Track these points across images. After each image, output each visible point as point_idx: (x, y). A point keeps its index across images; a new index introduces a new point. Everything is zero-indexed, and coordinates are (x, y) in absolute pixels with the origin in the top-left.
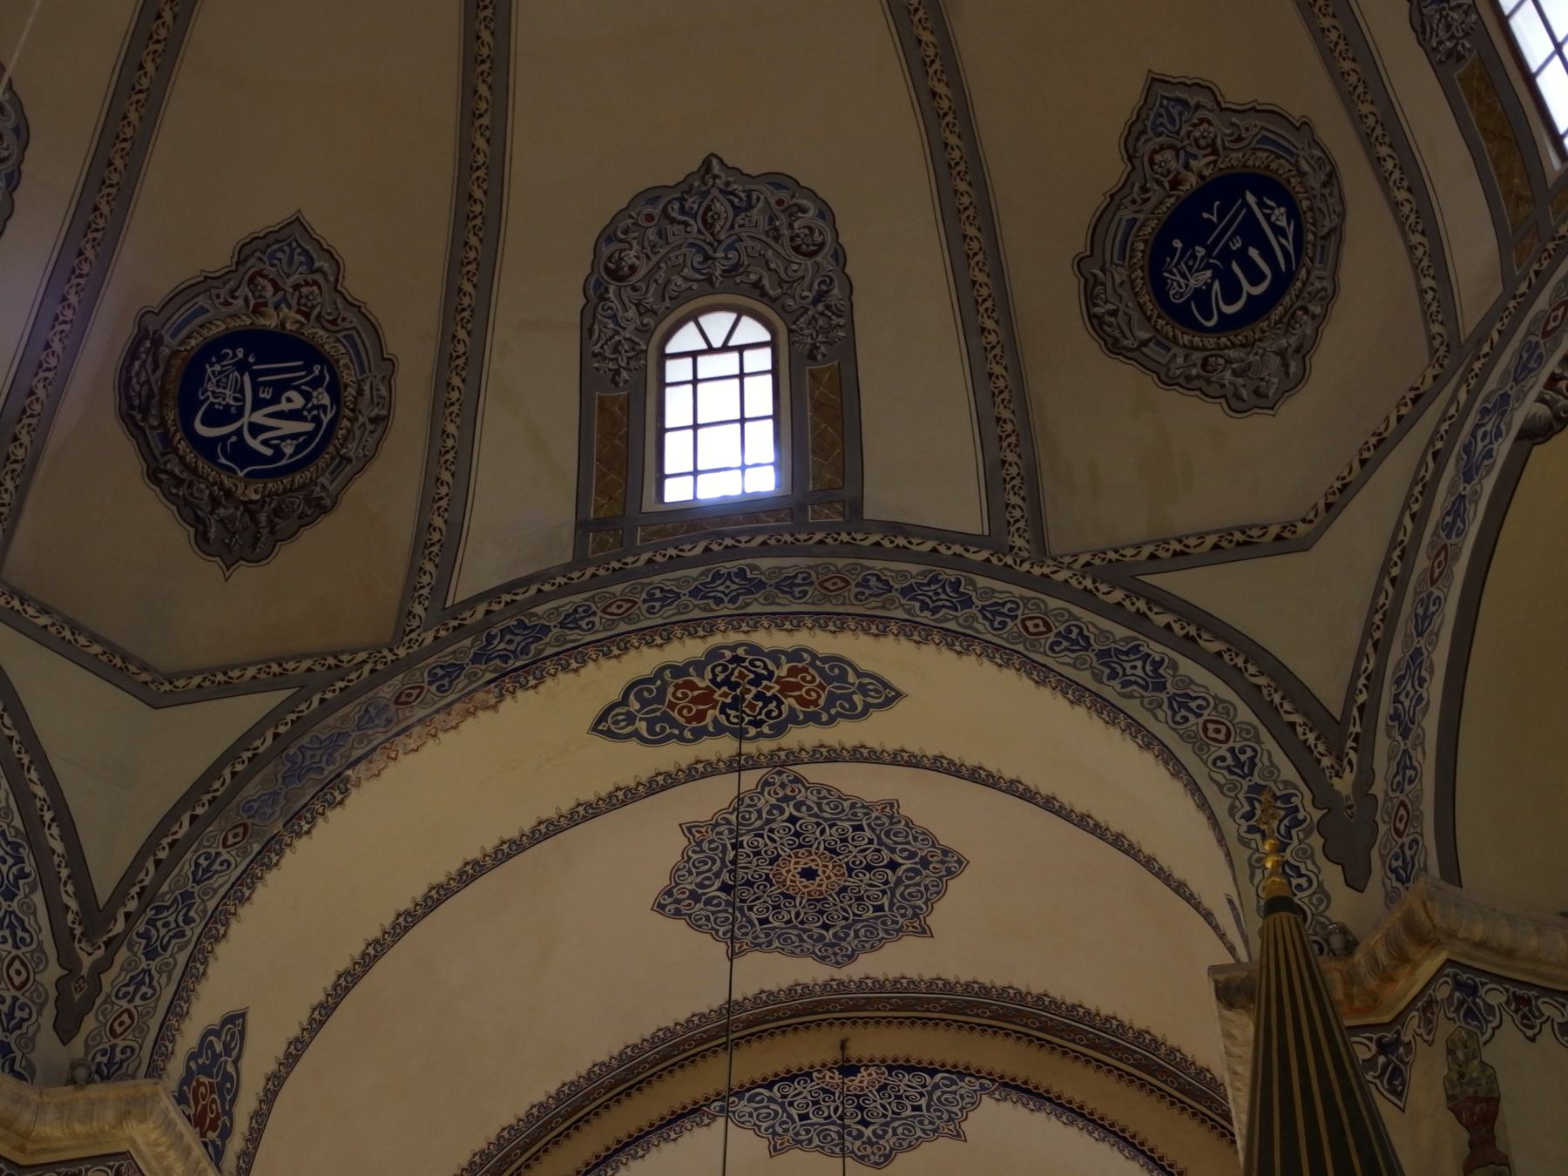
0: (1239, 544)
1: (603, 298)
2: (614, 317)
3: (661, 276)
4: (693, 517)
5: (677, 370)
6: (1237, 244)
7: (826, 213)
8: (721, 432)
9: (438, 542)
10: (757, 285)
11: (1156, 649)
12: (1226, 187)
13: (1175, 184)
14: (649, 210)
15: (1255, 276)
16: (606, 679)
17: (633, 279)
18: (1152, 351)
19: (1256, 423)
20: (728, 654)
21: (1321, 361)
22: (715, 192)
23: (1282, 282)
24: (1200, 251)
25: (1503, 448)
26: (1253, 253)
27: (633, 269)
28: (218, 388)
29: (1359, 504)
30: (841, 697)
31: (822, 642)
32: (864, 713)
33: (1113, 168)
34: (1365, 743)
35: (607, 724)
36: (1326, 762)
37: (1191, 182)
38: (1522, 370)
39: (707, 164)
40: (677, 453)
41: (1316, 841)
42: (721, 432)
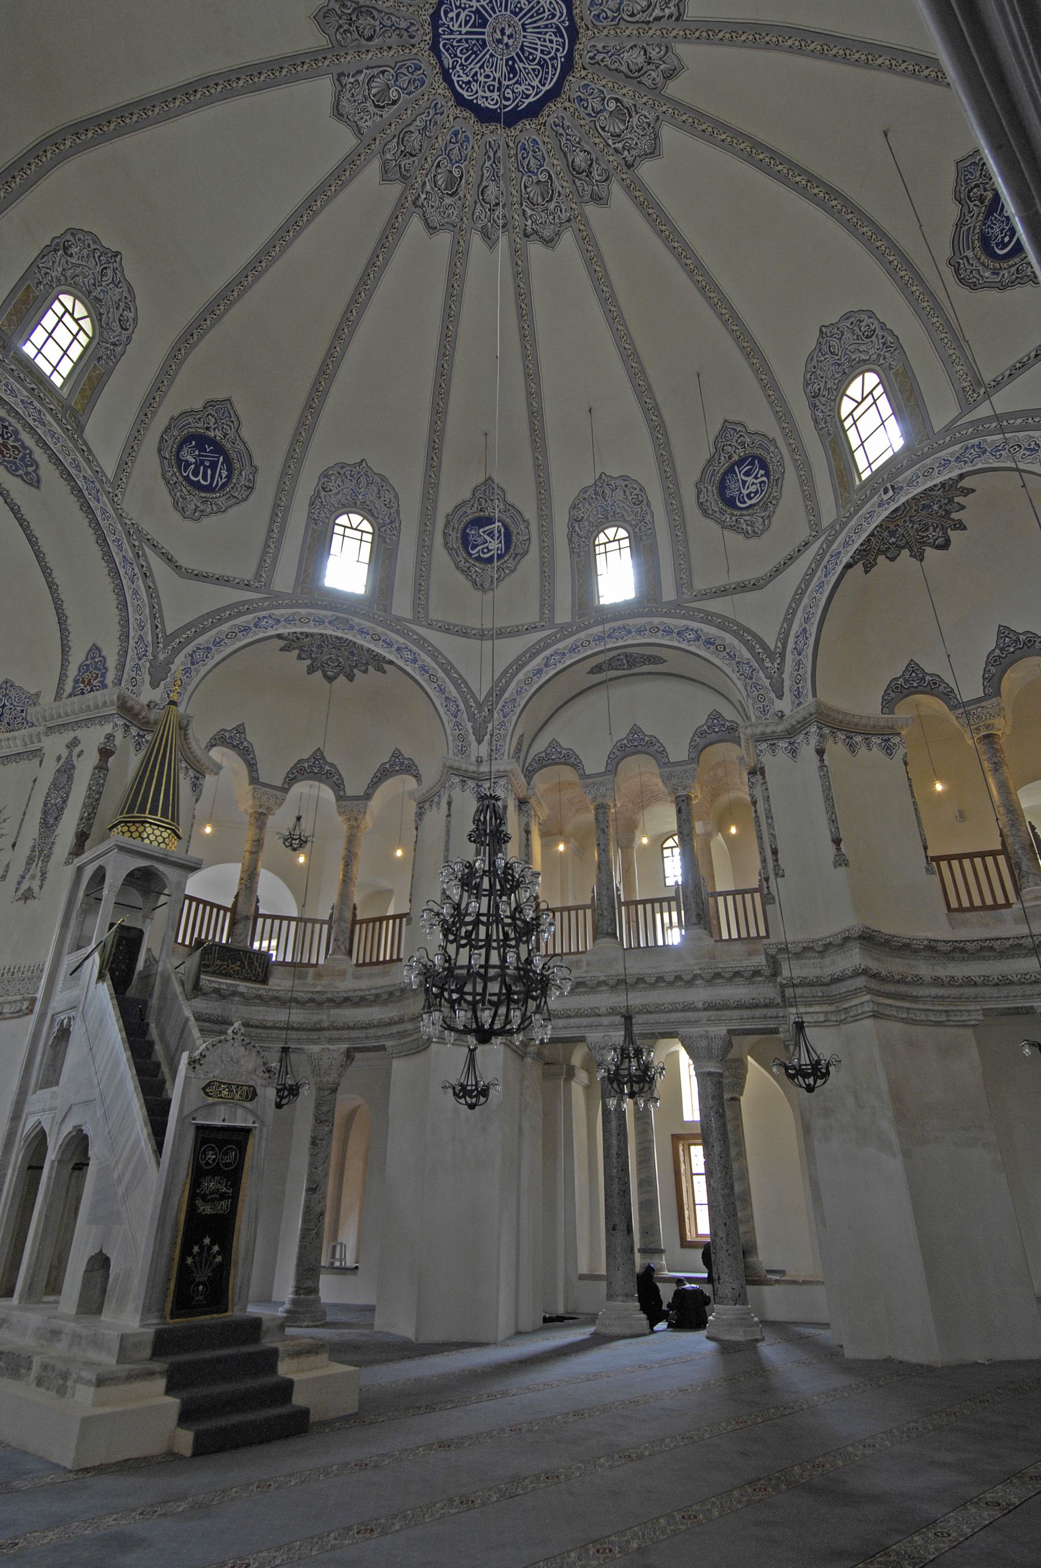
0: (169, 559)
1: (56, 251)
2: (54, 262)
3: (78, 270)
4: (29, 367)
5: (57, 307)
6: (207, 464)
7: (135, 320)
10: (101, 314)
11: (136, 570)
12: (219, 449)
13: (208, 429)
14: (91, 242)
15: (205, 478)
17: (69, 259)
18: (166, 461)
19: (178, 516)
20: (7, 424)
21: (205, 521)
22: (111, 265)
23: (209, 489)
24: (197, 453)
25: (271, 632)
26: (209, 471)
27: (71, 255)
29: (208, 588)
30: (17, 466)
31: (39, 455)
32: (17, 476)
33: (198, 405)
34: (176, 652)
36: (161, 645)
37: (211, 434)
38: (289, 620)
39: (117, 254)
40: (39, 336)
41: (148, 665)
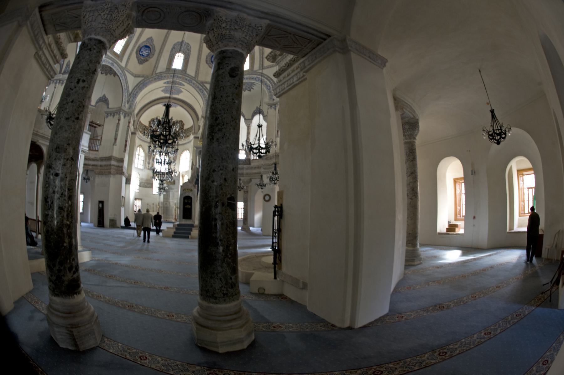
8: (178, 62)
9: (156, 67)
16: (165, 81)
28: (142, 50)
35: (164, 83)
42: (178, 62)
